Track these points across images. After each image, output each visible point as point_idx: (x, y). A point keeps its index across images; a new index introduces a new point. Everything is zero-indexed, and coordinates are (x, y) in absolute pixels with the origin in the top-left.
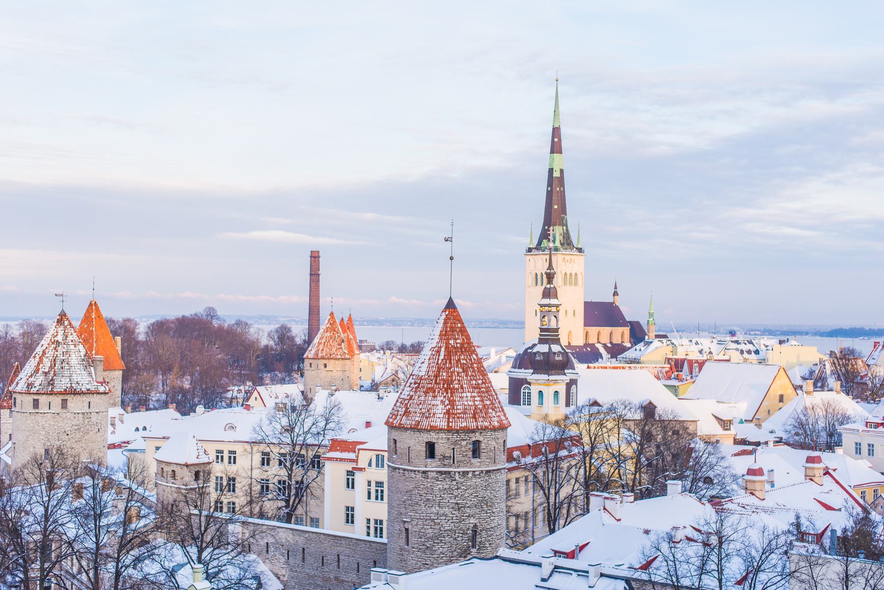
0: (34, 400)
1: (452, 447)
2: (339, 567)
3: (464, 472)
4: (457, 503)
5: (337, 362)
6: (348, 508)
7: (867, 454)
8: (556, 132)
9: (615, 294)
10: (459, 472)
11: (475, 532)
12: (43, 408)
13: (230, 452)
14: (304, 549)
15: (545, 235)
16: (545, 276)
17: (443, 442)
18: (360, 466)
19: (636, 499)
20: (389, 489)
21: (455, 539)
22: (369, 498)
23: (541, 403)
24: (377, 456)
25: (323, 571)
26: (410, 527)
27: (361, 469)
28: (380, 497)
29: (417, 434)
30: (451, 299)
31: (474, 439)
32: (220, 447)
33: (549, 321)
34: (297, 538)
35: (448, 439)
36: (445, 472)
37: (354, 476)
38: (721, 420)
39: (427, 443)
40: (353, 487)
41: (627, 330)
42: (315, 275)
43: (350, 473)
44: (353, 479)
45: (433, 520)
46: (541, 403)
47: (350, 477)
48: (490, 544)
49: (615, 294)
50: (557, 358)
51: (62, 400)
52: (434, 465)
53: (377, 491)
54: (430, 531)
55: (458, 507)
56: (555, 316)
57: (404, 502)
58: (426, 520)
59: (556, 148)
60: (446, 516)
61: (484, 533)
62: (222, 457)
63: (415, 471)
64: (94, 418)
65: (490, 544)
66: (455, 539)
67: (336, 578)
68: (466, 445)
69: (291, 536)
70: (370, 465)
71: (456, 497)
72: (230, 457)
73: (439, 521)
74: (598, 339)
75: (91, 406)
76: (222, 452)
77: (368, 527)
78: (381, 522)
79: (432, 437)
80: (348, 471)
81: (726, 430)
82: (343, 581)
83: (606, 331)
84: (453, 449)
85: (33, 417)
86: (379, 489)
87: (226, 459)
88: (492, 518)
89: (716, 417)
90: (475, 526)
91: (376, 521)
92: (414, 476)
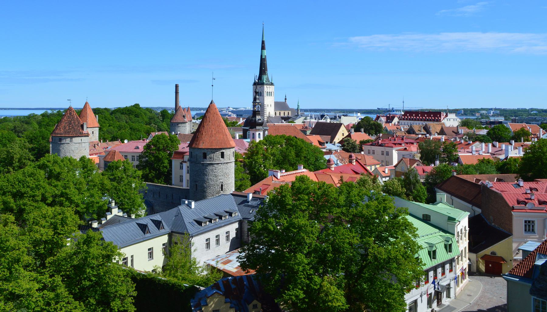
2: (173, 198)
6: (181, 176)
9: (286, 99)
11: (222, 185)
13: (137, 156)
14: (159, 192)
22: (188, 173)
27: (185, 162)
34: (157, 188)
37: (182, 164)
41: (290, 112)
43: (181, 164)
49: (286, 99)
61: (226, 185)
62: (134, 158)
71: (215, 172)
72: (137, 158)
74: (280, 114)
76: (134, 156)
77: (188, 183)
83: (282, 113)
87: (136, 159)
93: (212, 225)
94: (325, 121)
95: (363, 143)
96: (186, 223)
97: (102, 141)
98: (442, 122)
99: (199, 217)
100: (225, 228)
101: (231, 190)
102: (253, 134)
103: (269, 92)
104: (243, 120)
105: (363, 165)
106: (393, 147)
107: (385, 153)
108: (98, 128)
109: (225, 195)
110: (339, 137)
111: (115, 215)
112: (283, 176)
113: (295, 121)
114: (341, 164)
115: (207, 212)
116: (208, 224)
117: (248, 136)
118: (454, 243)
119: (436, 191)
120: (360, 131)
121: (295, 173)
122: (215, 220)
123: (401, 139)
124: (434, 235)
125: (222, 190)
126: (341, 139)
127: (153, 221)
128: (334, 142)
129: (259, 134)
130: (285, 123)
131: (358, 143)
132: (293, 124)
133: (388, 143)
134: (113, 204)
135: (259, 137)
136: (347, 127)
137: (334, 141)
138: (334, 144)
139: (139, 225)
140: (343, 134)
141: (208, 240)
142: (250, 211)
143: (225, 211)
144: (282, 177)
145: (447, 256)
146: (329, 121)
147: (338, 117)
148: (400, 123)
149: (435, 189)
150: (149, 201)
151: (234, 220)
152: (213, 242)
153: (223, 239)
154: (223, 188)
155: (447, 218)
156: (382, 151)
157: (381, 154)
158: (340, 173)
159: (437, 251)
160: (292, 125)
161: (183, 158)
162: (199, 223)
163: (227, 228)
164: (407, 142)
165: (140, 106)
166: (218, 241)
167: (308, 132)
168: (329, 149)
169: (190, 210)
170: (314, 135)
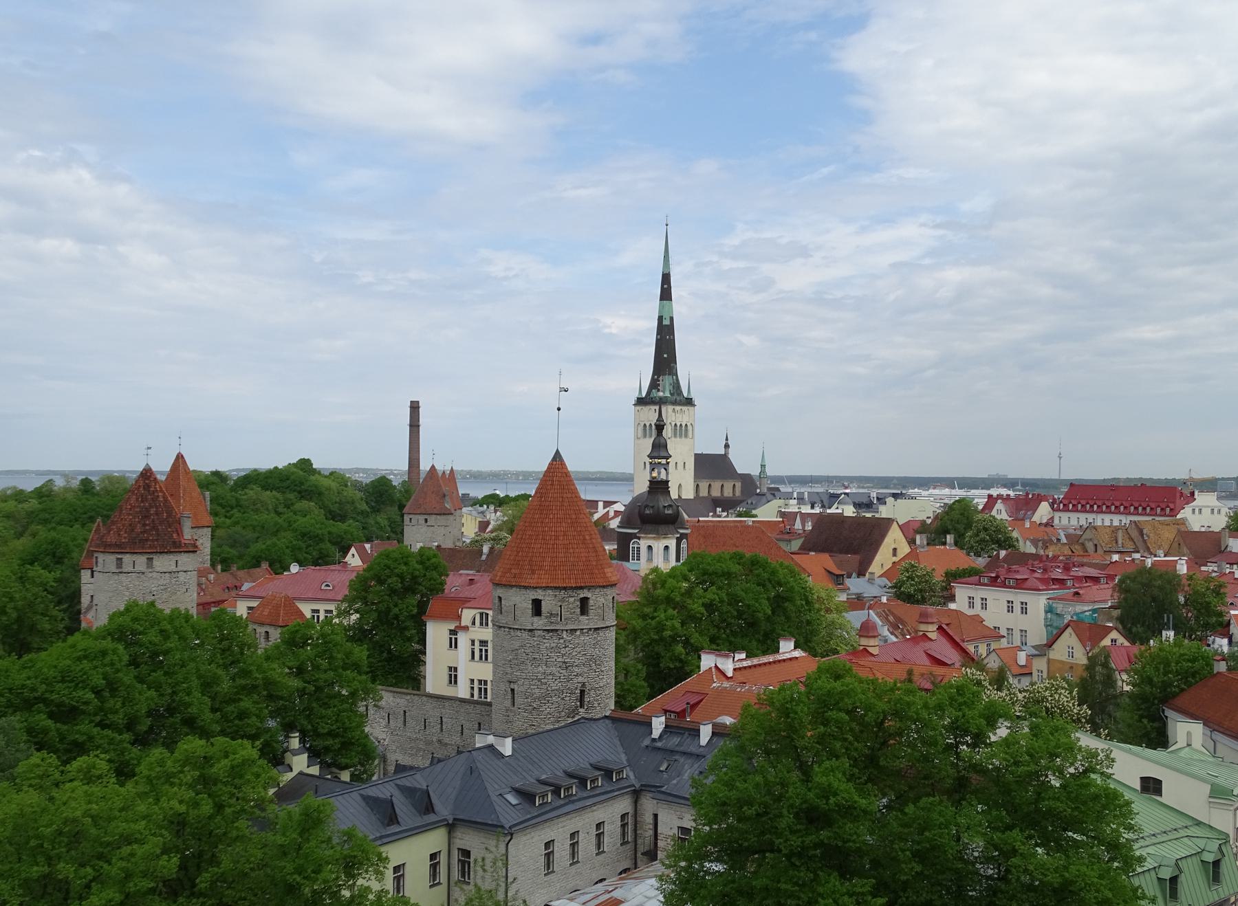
0: (118, 559)
1: (559, 604)
3: (571, 630)
4: (564, 662)
5: (438, 517)
6: (450, 668)
7: (980, 608)
8: (666, 278)
9: (727, 446)
10: (567, 630)
11: (582, 692)
12: (127, 567)
13: (327, 611)
15: (654, 385)
16: (654, 427)
17: (550, 599)
18: (463, 624)
19: (747, 656)
20: (494, 649)
21: (563, 699)
22: (473, 657)
23: (650, 559)
24: (481, 614)
25: (426, 735)
26: (515, 687)
27: (466, 628)
28: (484, 657)
29: (523, 591)
30: (557, 453)
31: (582, 596)
32: (315, 607)
33: (659, 473)
34: (398, 700)
35: (556, 596)
36: (552, 631)
38: (834, 574)
39: (534, 601)
40: (456, 647)
41: (738, 485)
42: (414, 425)
43: (453, 632)
44: (456, 639)
45: (540, 680)
46: (650, 559)
47: (453, 637)
48: (599, 704)
49: (727, 446)
50: (666, 512)
51: (148, 559)
52: (541, 622)
53: (481, 650)
54: (537, 691)
55: (566, 666)
56: (665, 469)
57: (510, 661)
58: (533, 680)
59: (666, 295)
60: (553, 675)
63: (521, 629)
64: (182, 576)
65: (599, 704)
66: (563, 699)
67: (440, 741)
68: (573, 601)
69: (391, 699)
70: (474, 623)
71: (563, 655)
73: (546, 680)
75: (179, 562)
76: (318, 611)
77: (472, 688)
78: (486, 682)
79: (539, 594)
80: (450, 630)
81: (839, 584)
82: (446, 744)
83: (716, 485)
84: (561, 606)
85: (116, 577)
86: (484, 648)
88: (601, 677)
89: (829, 572)
90: (584, 685)
91: (480, 681)
92: (519, 633)
93: (562, 802)
94: (839, 511)
95: (955, 576)
96: (491, 794)
97: (219, 567)
98: (1179, 517)
99: (527, 781)
100: (595, 813)
101: (606, 706)
102: (650, 548)
103: (681, 425)
104: (604, 508)
105: (958, 640)
106: (1039, 590)
107: (1017, 607)
108: (210, 529)
109: (591, 719)
110: (882, 560)
111: (301, 773)
112: (740, 669)
113: (754, 512)
114: (894, 639)
115: (544, 768)
116: (549, 801)
117: (633, 556)
118: (1226, 858)
119: (1166, 717)
120: (944, 544)
121: (774, 662)
122: (568, 788)
123: (1061, 565)
124: (1171, 836)
125: (582, 706)
126: (888, 566)
127: (404, 790)
128: (872, 573)
129: (667, 548)
130: (724, 517)
131: (938, 578)
132: (749, 520)
133: (1026, 577)
134: (295, 743)
135: (666, 559)
136: (911, 530)
137: (869, 571)
138: (871, 581)
139: (367, 799)
140: (895, 550)
141: (548, 845)
142: (661, 764)
143: (591, 765)
144: (738, 673)
145: (1209, 893)
146: (849, 511)
147: (878, 498)
148: (1056, 521)
149: (1163, 711)
150: (377, 739)
151: (619, 789)
152: (562, 851)
153: (587, 844)
154: (587, 699)
155: (1207, 788)
156: (1008, 602)
157: (1006, 608)
158: (893, 661)
159: (1182, 878)
160: (751, 524)
161: (459, 618)
162: (527, 796)
163: (600, 814)
164: (1081, 574)
165: (314, 467)
166: (574, 846)
167: (796, 545)
168: (857, 594)
169: (502, 760)
170: (813, 553)
